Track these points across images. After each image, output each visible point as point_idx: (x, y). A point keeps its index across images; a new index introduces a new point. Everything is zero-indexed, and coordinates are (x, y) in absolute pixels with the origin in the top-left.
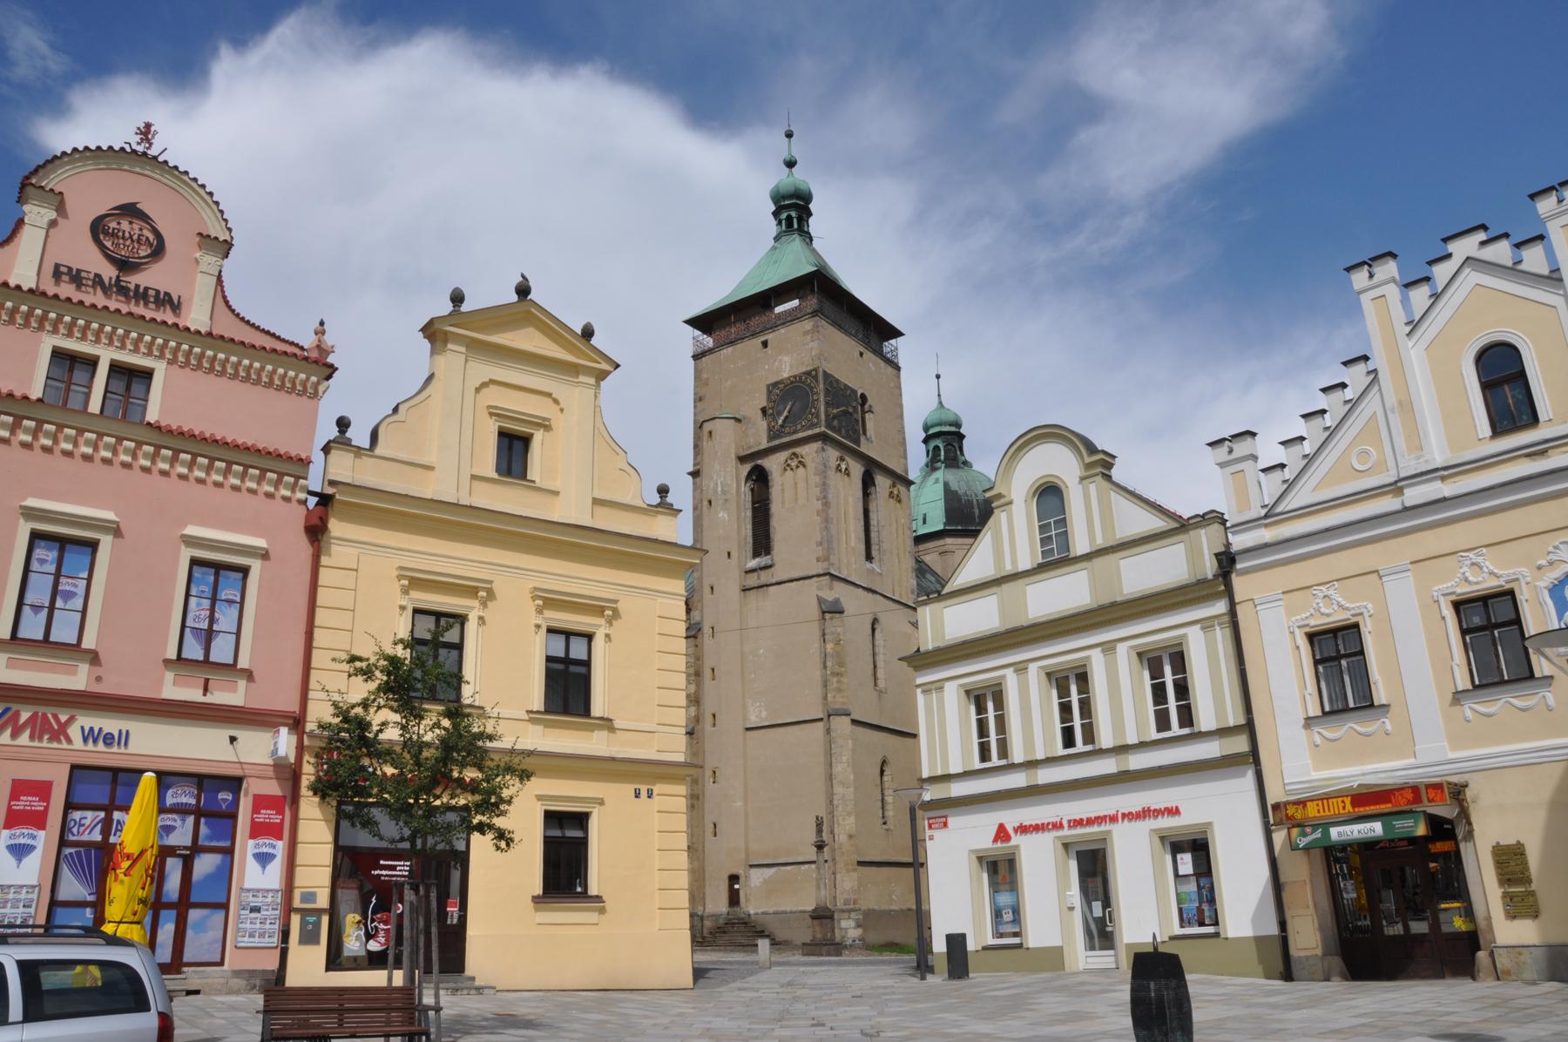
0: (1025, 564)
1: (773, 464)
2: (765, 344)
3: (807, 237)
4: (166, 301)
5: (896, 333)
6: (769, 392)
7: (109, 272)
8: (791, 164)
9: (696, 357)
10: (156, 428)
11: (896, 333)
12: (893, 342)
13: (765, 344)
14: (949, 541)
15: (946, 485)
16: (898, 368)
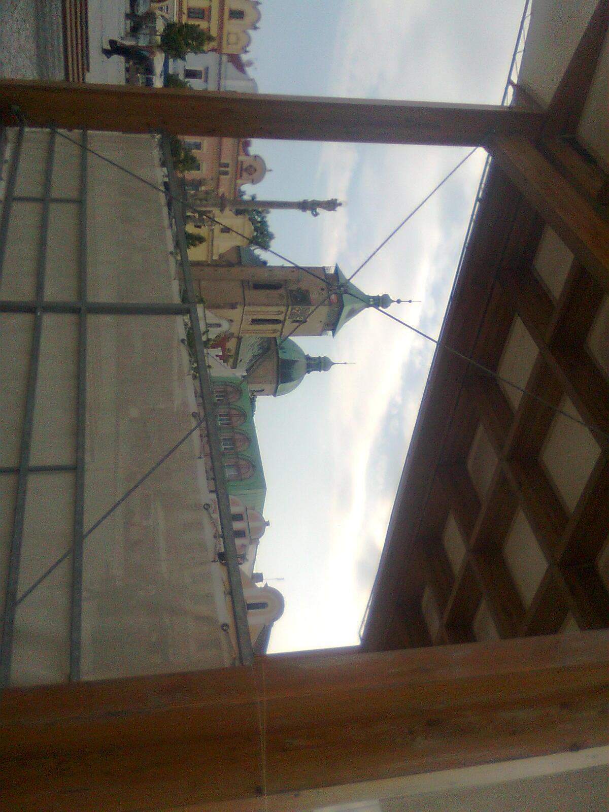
0: (207, 321)
1: (282, 291)
2: (323, 289)
3: (368, 306)
4: (241, 176)
5: (333, 335)
6: (306, 290)
7: (244, 167)
8: (399, 301)
9: (323, 269)
10: (218, 179)
11: (333, 335)
12: (330, 333)
13: (323, 289)
14: (275, 360)
15: (297, 361)
16: (321, 335)
